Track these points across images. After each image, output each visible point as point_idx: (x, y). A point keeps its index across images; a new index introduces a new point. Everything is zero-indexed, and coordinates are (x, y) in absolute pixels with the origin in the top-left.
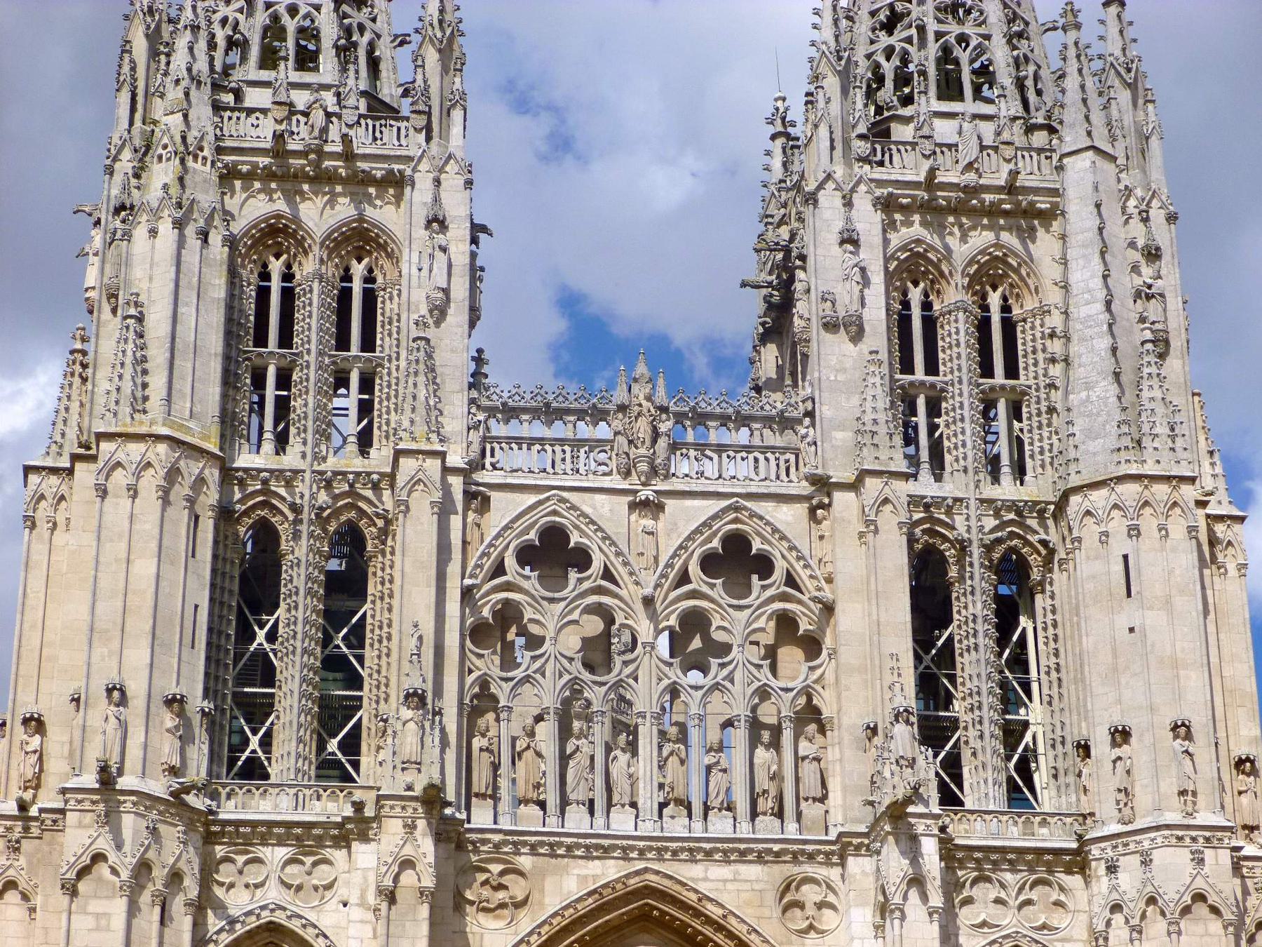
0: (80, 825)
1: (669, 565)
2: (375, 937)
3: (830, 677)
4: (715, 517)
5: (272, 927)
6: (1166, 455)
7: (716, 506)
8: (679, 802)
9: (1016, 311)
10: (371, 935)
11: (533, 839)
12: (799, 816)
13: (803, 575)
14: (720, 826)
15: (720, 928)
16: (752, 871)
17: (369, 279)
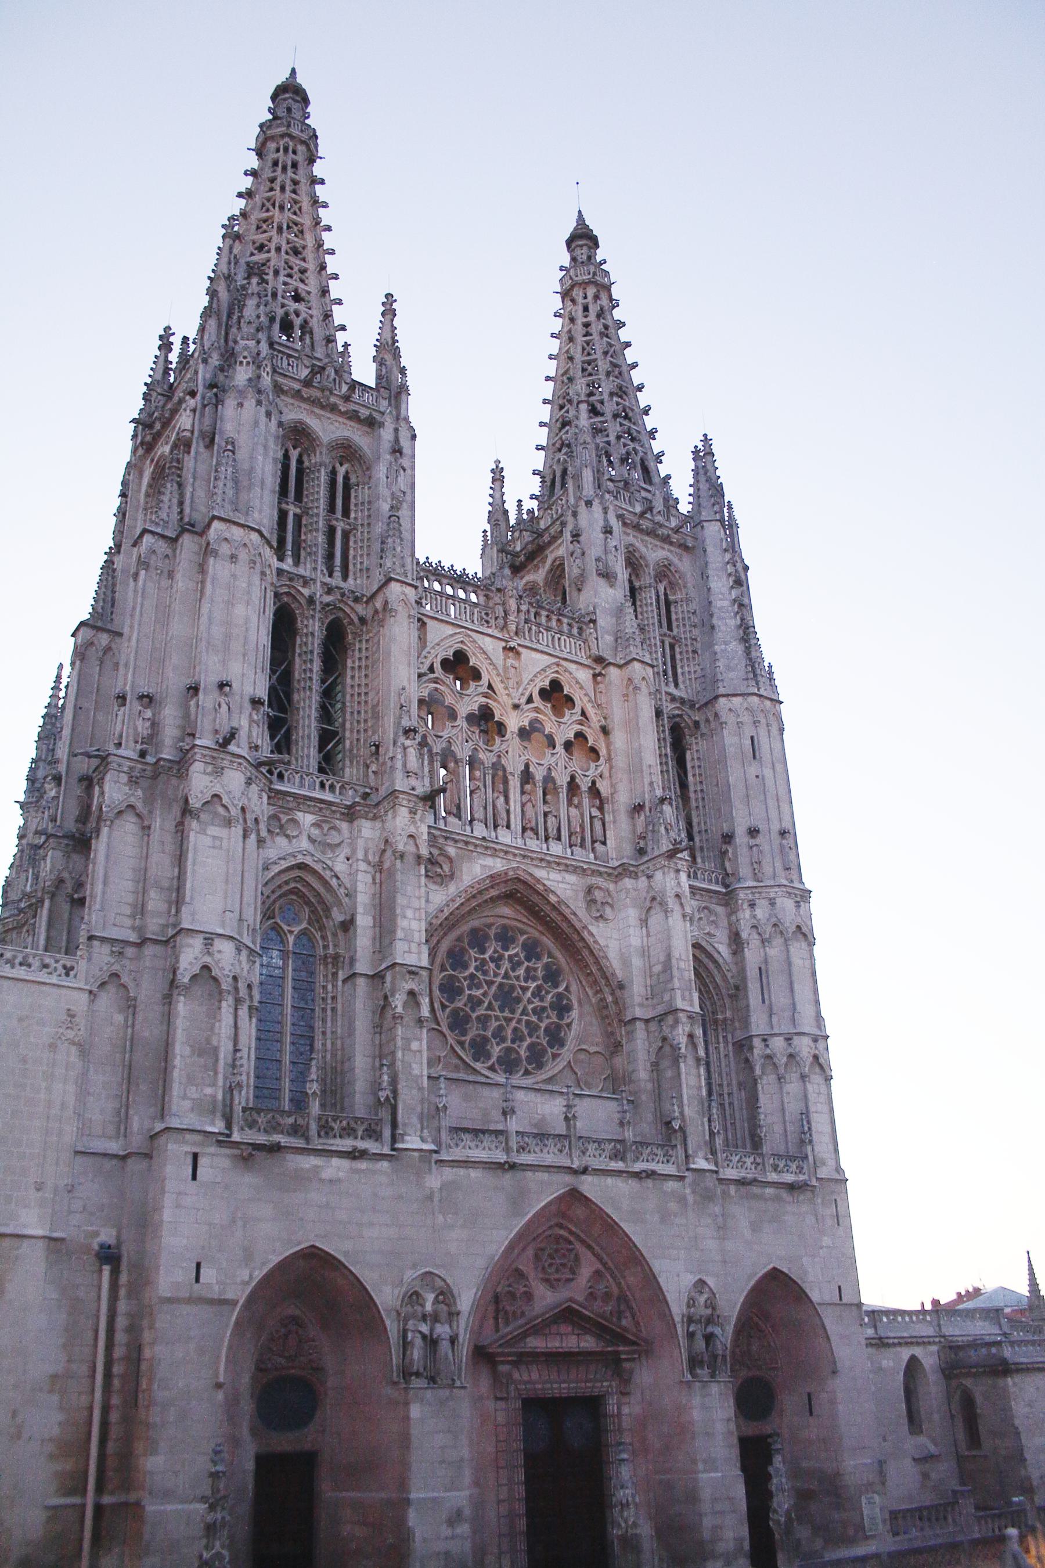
0: (205, 773)
1: (525, 689)
3: (606, 774)
4: (548, 666)
5: (302, 866)
6: (768, 688)
7: (547, 660)
8: (532, 829)
9: (671, 598)
10: (371, 881)
11: (457, 837)
12: (593, 849)
13: (591, 711)
14: (556, 848)
15: (554, 907)
16: (572, 878)
17: (346, 478)
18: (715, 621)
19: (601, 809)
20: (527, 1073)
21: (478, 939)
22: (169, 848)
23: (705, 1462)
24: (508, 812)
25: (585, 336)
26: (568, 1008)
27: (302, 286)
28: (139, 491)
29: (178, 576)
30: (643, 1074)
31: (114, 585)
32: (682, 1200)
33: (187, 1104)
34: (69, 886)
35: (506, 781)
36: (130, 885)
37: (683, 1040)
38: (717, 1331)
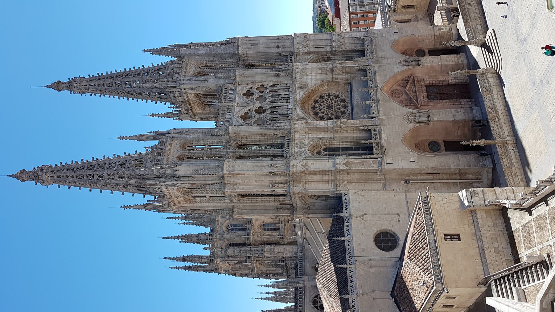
2: (311, 134)
13: (250, 86)
18: (214, 53)
19: (277, 84)
20: (347, 103)
21: (316, 114)
22: (312, 176)
23: (439, 63)
24: (283, 106)
25: (104, 86)
26: (329, 94)
27: (117, 163)
28: (187, 207)
29: (238, 181)
30: (347, 76)
31: (218, 209)
32: (379, 66)
33: (375, 166)
34: (305, 210)
35: (275, 107)
36: (321, 185)
37: (340, 65)
38: (409, 60)
